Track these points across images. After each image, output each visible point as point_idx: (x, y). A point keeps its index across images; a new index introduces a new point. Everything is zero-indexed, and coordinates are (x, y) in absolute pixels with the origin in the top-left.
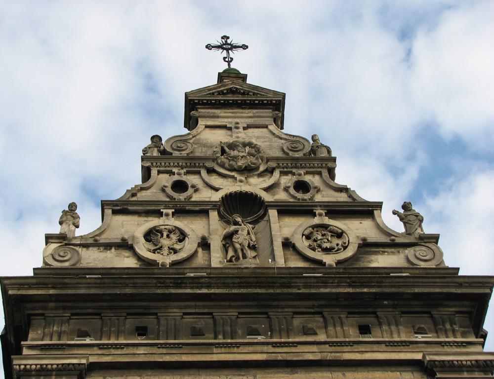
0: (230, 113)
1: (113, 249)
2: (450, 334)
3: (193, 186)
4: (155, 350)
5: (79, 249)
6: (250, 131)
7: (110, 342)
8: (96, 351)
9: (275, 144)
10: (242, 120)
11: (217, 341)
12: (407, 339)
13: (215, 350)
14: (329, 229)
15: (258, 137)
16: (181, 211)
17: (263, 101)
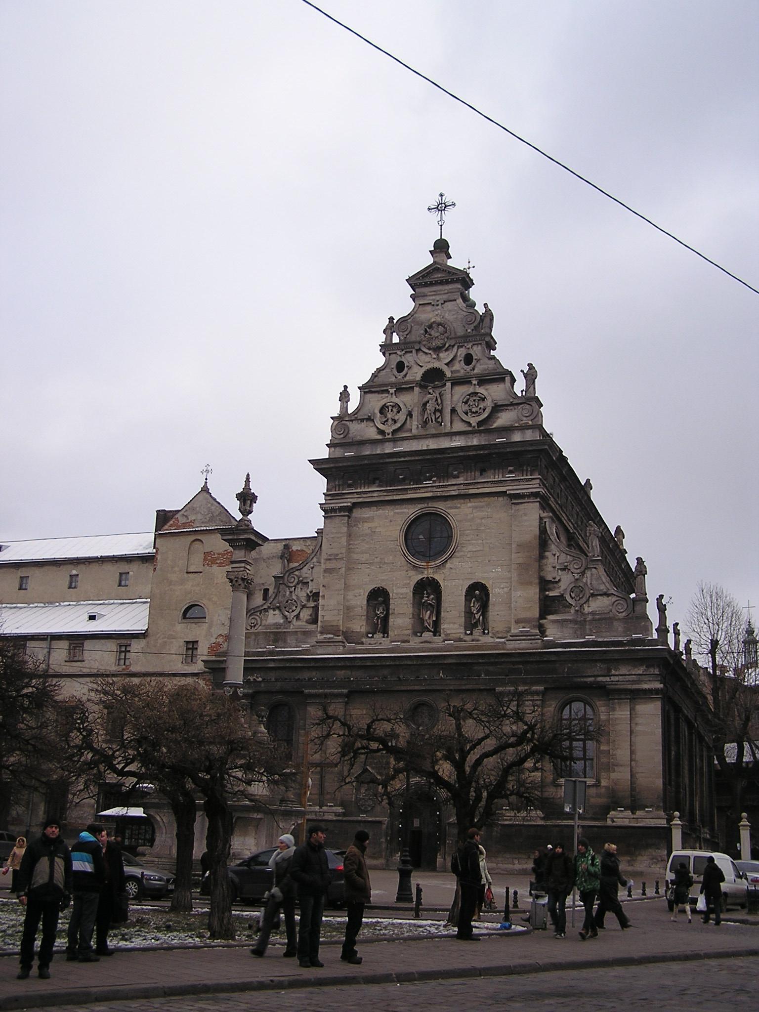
0: (434, 291)
2: (525, 473)
3: (407, 366)
4: (381, 494)
5: (348, 423)
6: (446, 304)
9: (459, 317)
10: (441, 297)
11: (409, 487)
12: (503, 479)
13: (409, 492)
14: (479, 394)
15: (450, 311)
17: (453, 279)
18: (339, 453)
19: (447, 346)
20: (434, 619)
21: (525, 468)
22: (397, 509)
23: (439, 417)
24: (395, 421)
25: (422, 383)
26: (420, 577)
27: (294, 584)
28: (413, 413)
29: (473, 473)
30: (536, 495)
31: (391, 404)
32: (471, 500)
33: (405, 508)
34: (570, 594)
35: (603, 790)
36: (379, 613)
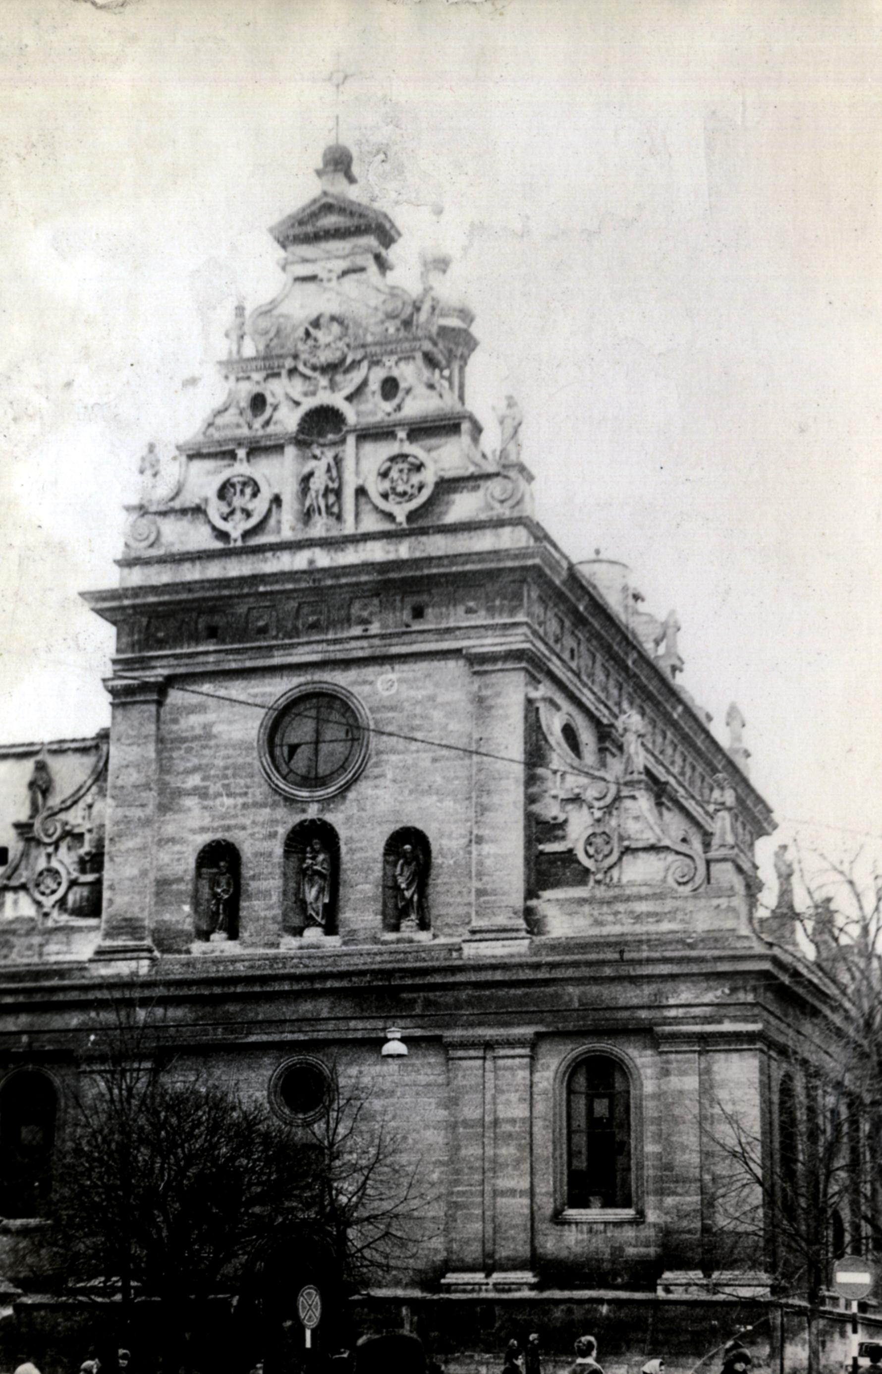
1: (189, 516)
4: (222, 656)
7: (185, 650)
8: (173, 662)
11: (274, 642)
13: (276, 653)
14: (410, 459)
16: (256, 449)
18: (137, 577)
19: (349, 361)
20: (327, 900)
21: (497, 603)
22: (253, 687)
23: (333, 505)
24: (248, 514)
25: (301, 437)
26: (298, 818)
27: (55, 837)
28: (283, 497)
29: (398, 614)
30: (517, 655)
31: (241, 479)
32: (397, 667)
33: (270, 685)
34: (587, 852)
35: (650, 1233)
36: (219, 890)
